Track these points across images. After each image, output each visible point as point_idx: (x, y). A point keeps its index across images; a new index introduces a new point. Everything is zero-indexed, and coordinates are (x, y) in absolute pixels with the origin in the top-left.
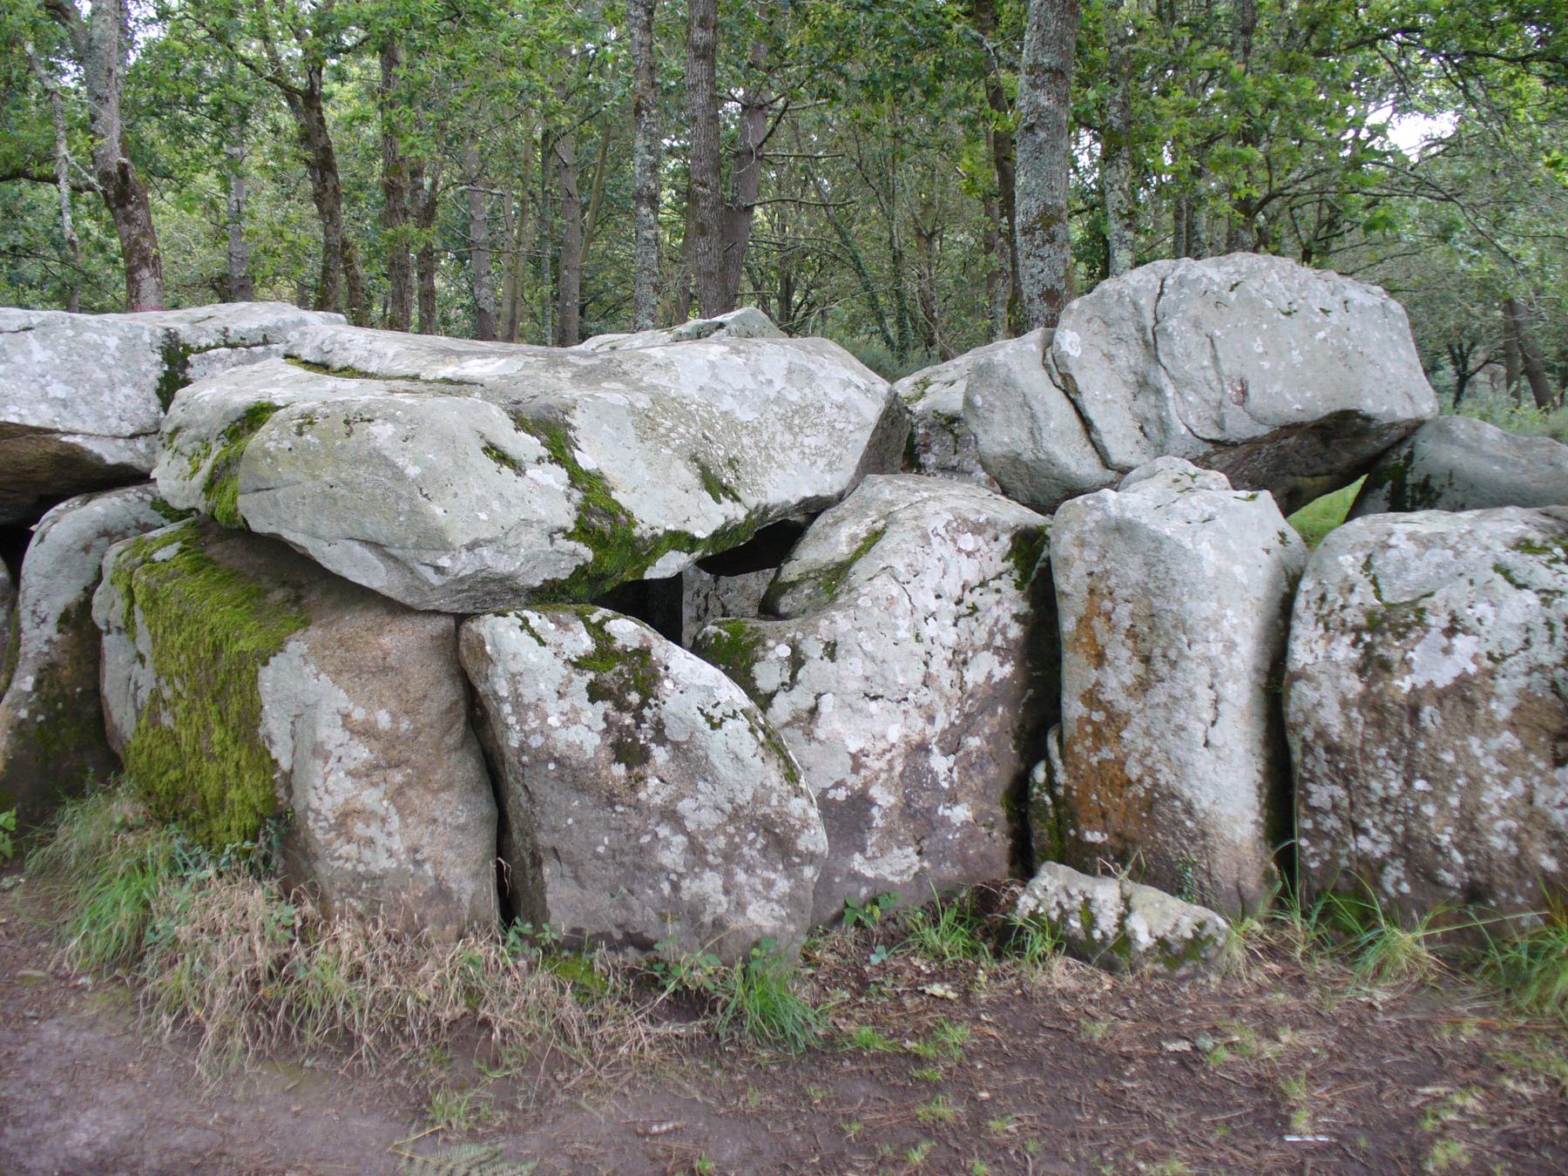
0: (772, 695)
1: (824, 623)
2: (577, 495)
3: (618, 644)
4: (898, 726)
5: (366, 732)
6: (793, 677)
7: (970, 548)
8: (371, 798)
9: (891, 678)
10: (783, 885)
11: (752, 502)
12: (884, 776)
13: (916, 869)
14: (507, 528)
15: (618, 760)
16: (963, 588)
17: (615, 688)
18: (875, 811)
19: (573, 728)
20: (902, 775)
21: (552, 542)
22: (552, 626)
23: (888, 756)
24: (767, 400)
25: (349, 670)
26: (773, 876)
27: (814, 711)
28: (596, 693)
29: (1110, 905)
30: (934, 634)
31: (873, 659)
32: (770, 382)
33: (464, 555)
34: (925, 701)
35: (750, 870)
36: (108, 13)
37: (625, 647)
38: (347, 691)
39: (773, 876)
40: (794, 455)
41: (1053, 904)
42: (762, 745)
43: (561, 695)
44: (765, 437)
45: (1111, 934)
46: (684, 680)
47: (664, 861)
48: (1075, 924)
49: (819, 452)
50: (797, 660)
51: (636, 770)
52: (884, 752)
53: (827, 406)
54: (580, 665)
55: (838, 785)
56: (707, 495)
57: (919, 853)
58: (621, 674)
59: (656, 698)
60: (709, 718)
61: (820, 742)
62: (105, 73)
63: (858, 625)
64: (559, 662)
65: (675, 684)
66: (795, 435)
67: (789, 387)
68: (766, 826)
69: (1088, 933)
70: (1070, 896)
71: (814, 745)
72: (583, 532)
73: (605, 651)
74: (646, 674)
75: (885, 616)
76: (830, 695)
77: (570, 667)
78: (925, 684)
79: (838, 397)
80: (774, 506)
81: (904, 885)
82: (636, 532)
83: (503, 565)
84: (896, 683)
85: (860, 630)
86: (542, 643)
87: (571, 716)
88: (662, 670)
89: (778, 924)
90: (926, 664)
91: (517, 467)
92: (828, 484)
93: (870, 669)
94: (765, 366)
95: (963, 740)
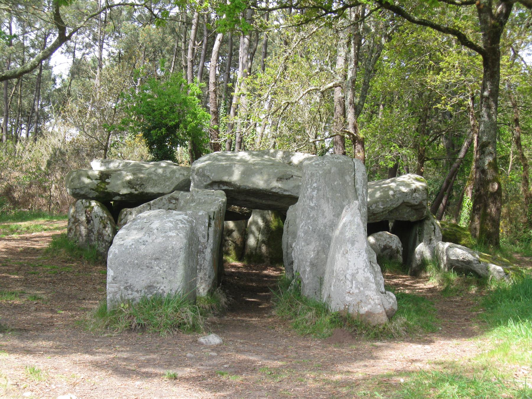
11: (141, 190)
92: (167, 190)
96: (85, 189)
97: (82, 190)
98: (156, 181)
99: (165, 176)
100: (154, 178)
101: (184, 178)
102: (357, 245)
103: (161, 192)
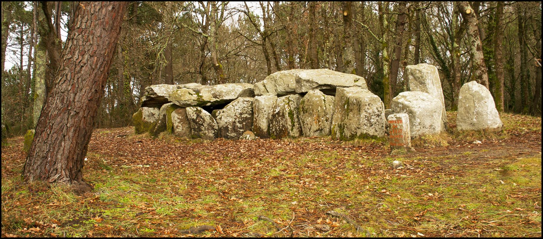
5: (179, 119)
8: (180, 125)
25: (178, 113)
68: (211, 126)
73: (197, 110)
74: (200, 112)
83: (188, 103)
92: (234, 98)
102: (490, 99)
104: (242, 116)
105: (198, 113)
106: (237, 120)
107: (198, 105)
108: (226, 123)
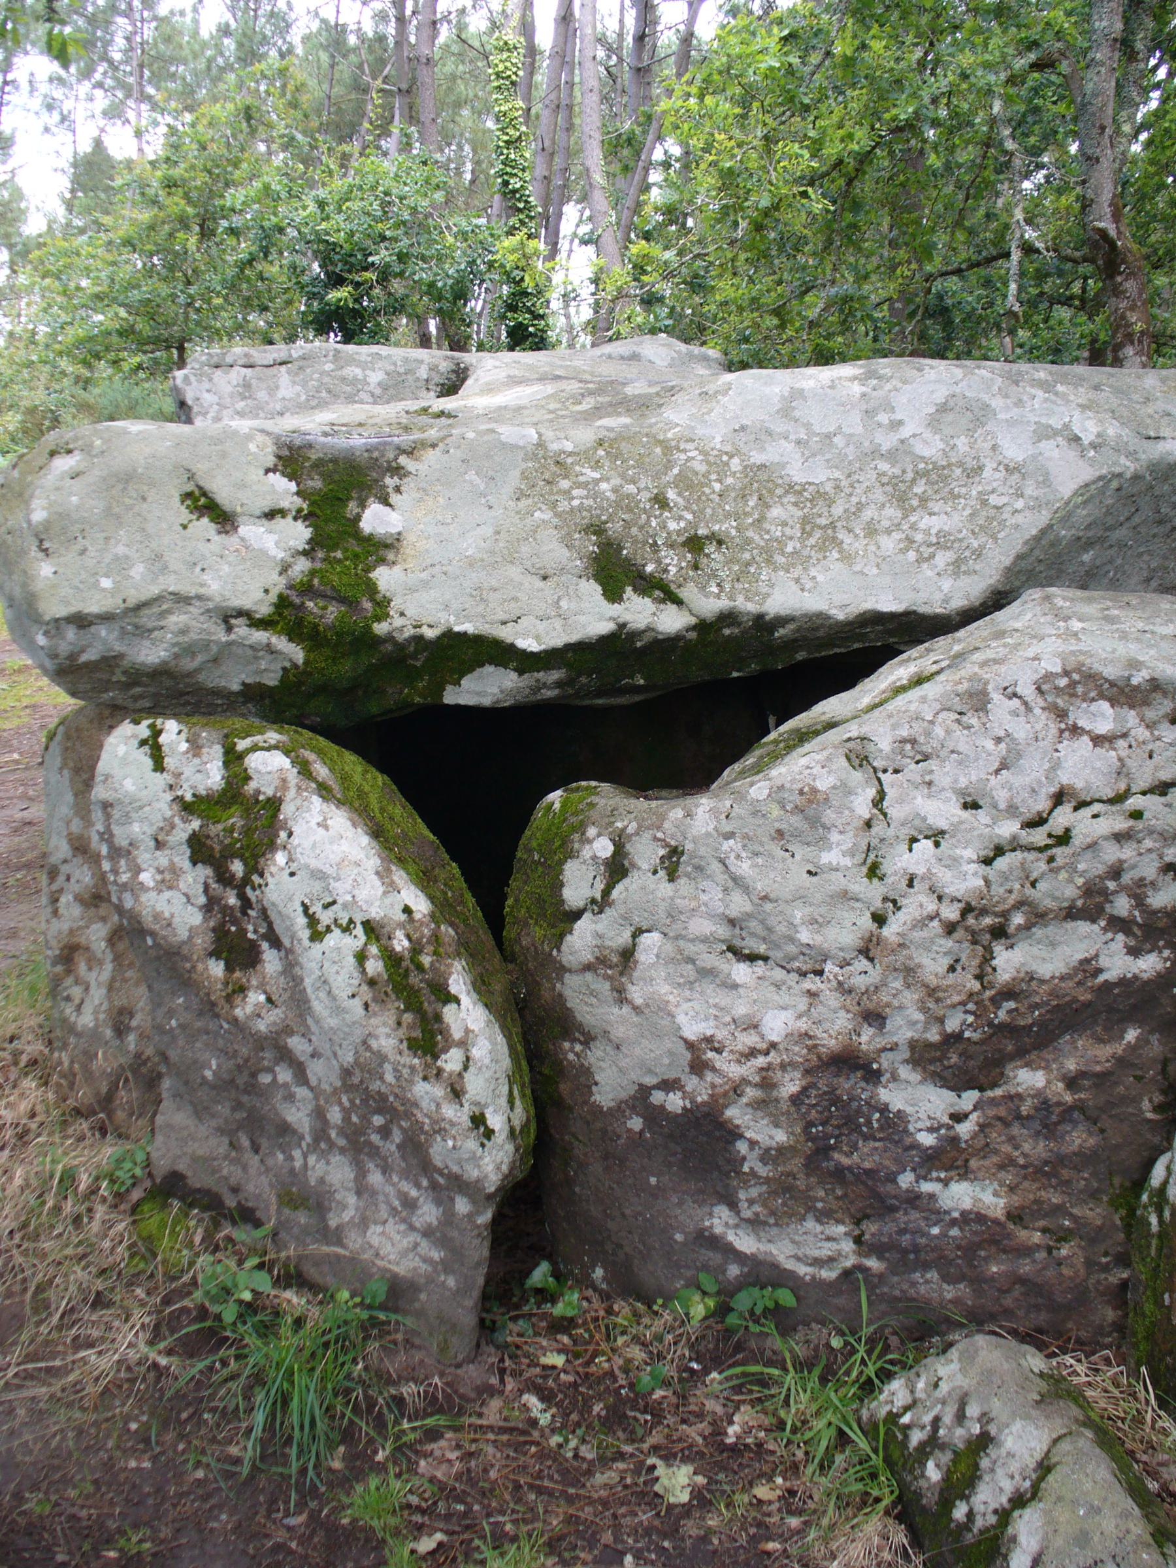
0: (577, 915)
1: (677, 813)
2: (302, 565)
3: (252, 786)
4: (787, 1016)
6: (606, 892)
7: (1103, 727)
9: (781, 929)
10: (428, 1213)
12: (751, 1093)
13: (848, 1264)
14: (131, 602)
15: (215, 954)
16: (1059, 798)
17: (217, 848)
18: (742, 1147)
19: (167, 894)
20: (795, 1100)
21: (229, 629)
22: (184, 746)
23: (761, 1061)
24: (876, 453)
26: (414, 1193)
27: (628, 955)
28: (199, 849)
29: (1014, 1467)
30: (920, 870)
31: (746, 890)
32: (896, 425)
33: (71, 633)
34: (860, 982)
35: (385, 1170)
36: (1103, 64)
37: (258, 792)
38: (76, 795)
39: (414, 1193)
40: (889, 544)
41: (927, 1419)
42: (372, 983)
43: (159, 845)
44: (838, 510)
45: (979, 1523)
46: (306, 858)
47: (289, 1119)
48: (933, 1473)
49: (942, 542)
50: (617, 868)
51: (238, 974)
52: (752, 1053)
53: (990, 465)
54: (187, 808)
55: (668, 1085)
56: (592, 589)
57: (858, 1240)
58: (231, 830)
59: (262, 875)
60: (312, 921)
61: (636, 1009)
62: (1096, 131)
63: (727, 827)
64: (169, 797)
65: (290, 860)
66: (907, 512)
67: (927, 435)
69: (947, 1504)
70: (960, 1417)
71: (626, 1009)
72: (285, 615)
75: (796, 821)
76: (655, 936)
77: (175, 807)
78: (865, 952)
79: (1015, 450)
80: (781, 621)
81: (817, 1283)
82: (380, 628)
84: (792, 940)
85: (729, 836)
86: (159, 766)
87: (168, 876)
88: (283, 834)
89: (424, 1267)
90: (880, 920)
91: (224, 519)
92: (938, 590)
93: (739, 904)
94: (901, 400)
95: (1009, 1071)
96: (176, 620)
97: (142, 632)
98: (820, 496)
99: (891, 456)
100: (797, 473)
101: (1087, 473)
103: (888, 604)
104: (1008, 962)
105: (234, 836)
106: (907, 1023)
107: (280, 704)
108: (699, 1056)
